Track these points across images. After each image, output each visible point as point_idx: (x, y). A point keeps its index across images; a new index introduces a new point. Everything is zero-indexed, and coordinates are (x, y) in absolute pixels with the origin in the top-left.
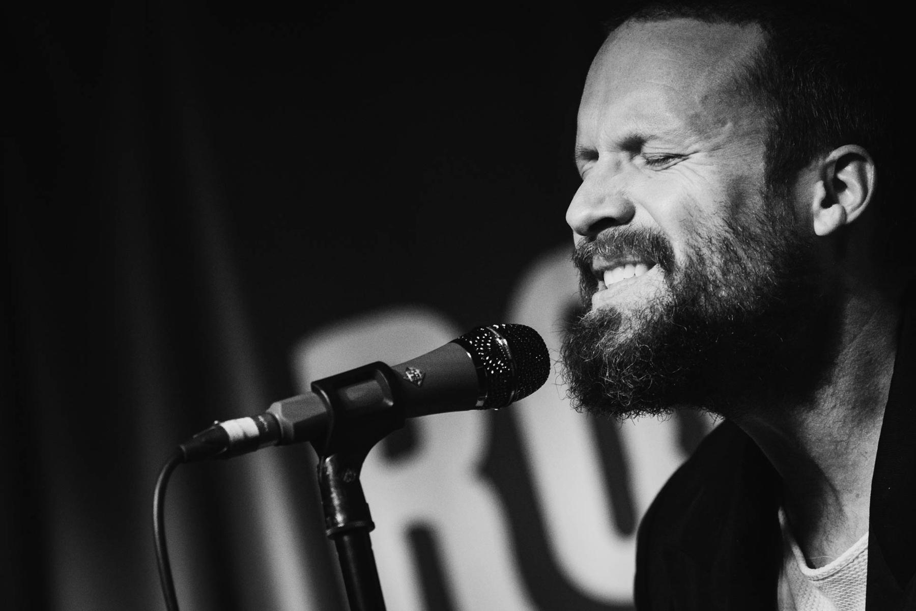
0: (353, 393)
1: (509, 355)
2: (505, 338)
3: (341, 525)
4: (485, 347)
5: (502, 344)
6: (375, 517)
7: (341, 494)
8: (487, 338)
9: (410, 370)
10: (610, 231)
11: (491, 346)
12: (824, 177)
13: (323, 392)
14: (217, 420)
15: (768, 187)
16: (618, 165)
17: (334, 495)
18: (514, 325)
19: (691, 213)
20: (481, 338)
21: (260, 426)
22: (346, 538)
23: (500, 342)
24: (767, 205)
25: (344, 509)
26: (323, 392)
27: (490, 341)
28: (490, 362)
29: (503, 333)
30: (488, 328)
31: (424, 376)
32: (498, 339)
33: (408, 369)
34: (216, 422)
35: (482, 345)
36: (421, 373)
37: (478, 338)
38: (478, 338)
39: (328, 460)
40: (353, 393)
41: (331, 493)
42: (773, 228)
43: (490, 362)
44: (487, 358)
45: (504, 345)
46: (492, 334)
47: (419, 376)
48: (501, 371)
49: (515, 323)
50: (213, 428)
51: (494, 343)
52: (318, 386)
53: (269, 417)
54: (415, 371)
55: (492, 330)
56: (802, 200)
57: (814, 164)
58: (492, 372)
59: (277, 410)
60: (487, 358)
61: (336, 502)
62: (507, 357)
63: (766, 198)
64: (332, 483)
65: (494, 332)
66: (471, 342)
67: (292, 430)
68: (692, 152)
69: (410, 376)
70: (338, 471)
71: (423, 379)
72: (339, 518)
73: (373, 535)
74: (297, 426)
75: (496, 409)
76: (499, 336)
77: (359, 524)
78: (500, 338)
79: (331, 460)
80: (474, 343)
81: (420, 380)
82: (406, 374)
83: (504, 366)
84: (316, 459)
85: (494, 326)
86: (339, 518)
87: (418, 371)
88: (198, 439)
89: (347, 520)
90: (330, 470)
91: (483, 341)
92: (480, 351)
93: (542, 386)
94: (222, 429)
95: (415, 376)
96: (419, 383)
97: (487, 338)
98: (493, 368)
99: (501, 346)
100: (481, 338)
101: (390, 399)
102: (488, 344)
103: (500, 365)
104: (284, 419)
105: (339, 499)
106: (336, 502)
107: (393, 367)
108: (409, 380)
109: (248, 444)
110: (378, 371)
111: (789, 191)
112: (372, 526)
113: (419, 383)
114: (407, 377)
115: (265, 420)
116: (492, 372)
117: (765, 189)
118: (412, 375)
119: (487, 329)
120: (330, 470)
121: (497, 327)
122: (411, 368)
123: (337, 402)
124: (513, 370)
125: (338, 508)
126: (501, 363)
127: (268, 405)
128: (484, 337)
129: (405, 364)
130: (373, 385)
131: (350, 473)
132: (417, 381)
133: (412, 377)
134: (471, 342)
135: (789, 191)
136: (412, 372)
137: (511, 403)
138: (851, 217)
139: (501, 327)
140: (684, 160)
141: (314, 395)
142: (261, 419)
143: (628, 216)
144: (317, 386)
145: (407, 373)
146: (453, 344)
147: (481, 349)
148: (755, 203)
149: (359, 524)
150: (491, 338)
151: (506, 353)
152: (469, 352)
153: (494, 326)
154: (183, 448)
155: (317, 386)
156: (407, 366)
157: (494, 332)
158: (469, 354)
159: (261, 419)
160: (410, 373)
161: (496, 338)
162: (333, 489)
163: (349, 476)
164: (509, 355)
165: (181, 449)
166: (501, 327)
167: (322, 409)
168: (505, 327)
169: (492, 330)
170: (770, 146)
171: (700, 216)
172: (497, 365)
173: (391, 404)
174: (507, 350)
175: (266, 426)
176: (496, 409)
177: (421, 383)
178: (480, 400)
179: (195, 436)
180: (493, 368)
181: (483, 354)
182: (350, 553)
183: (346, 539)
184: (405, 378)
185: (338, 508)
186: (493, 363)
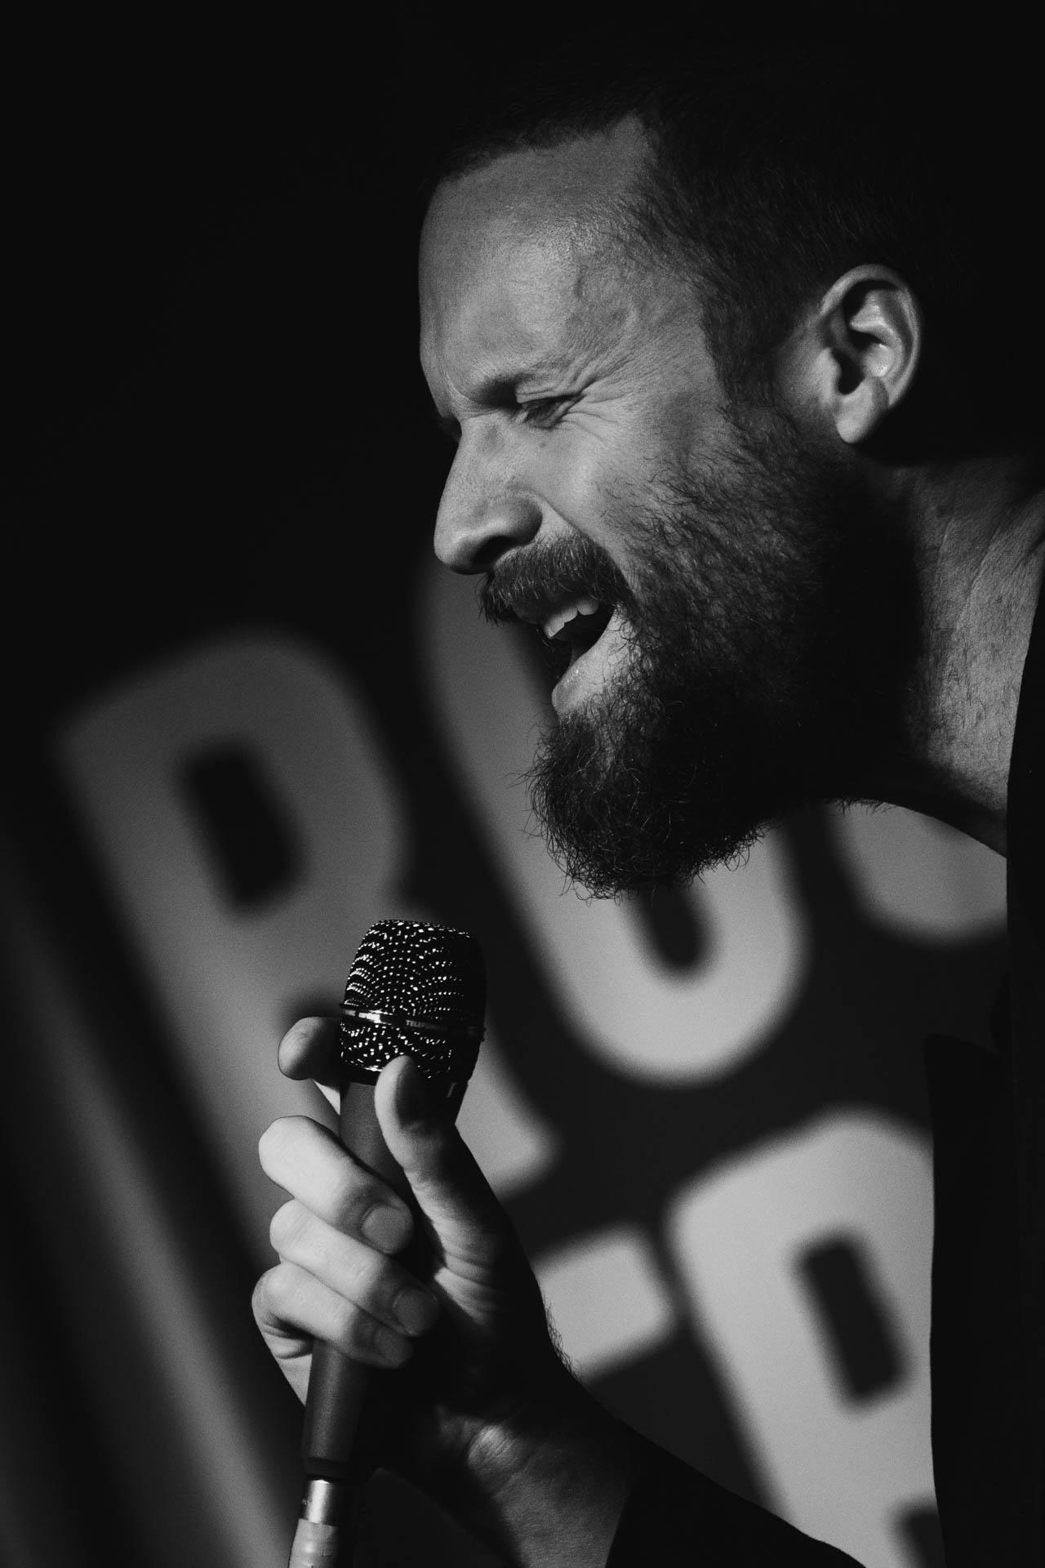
24: (740, 427)
42: (765, 464)
68: (584, 384)
117: (726, 403)
148: (715, 432)
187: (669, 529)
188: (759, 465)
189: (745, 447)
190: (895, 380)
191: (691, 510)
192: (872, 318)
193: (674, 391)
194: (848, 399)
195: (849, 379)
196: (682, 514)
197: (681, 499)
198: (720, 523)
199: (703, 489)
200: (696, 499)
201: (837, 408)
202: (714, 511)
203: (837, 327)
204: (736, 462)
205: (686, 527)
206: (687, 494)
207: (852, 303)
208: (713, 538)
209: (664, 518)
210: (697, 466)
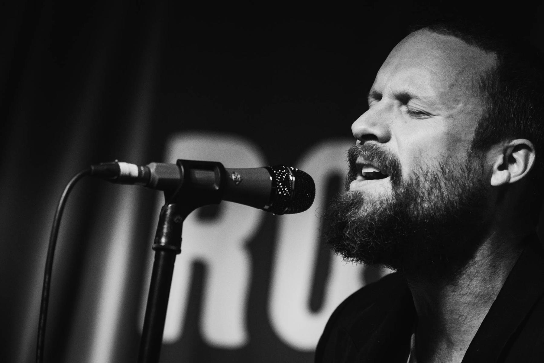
0: (199, 174)
1: (293, 187)
2: (295, 177)
3: (163, 244)
4: (282, 177)
5: (291, 179)
6: (183, 247)
7: (169, 228)
8: (285, 173)
9: (235, 174)
11: (285, 178)
13: (182, 168)
14: (116, 159)
17: (165, 226)
18: (302, 171)
20: (281, 172)
21: (140, 172)
22: (162, 253)
23: (291, 178)
24: (469, 161)
25: (168, 236)
26: (182, 168)
27: (285, 175)
28: (281, 187)
29: (295, 173)
30: (287, 167)
31: (242, 180)
32: (290, 176)
33: (234, 173)
34: (116, 161)
35: (280, 176)
36: (241, 178)
37: (280, 171)
38: (280, 171)
39: (170, 206)
40: (199, 174)
41: (164, 224)
43: (281, 187)
44: (280, 184)
45: (293, 180)
46: (288, 172)
47: (239, 179)
48: (285, 194)
49: (303, 171)
50: (113, 163)
51: (287, 177)
52: (180, 162)
53: (147, 169)
54: (237, 175)
55: (289, 169)
58: (280, 193)
59: (153, 167)
60: (280, 184)
61: (165, 230)
62: (292, 187)
63: (469, 156)
64: (167, 219)
65: (290, 171)
66: (275, 172)
67: (156, 182)
69: (233, 177)
70: (173, 214)
71: (240, 182)
72: (163, 240)
73: (178, 257)
74: (161, 181)
75: (274, 214)
76: (292, 174)
77: (173, 248)
78: (292, 176)
79: (171, 207)
80: (276, 173)
81: (239, 181)
82: (232, 175)
83: (288, 192)
84: (163, 203)
85: (291, 168)
86: (163, 240)
87: (239, 176)
88: (103, 166)
89: (167, 243)
90: (169, 212)
91: (282, 174)
92: (278, 178)
93: (304, 212)
94: (118, 167)
95: (237, 178)
96: (237, 183)
97: (285, 173)
98: (281, 190)
99: (291, 180)
100: (281, 172)
101: (218, 185)
102: (284, 177)
103: (286, 190)
104: (155, 174)
105: (168, 230)
106: (165, 230)
107: (227, 168)
108: (232, 179)
109: (129, 179)
110: (218, 168)
112: (179, 251)
113: (237, 183)
114: (232, 177)
115: (144, 170)
116: (280, 193)
117: (470, 151)
118: (235, 177)
119: (287, 168)
120: (169, 212)
121: (293, 169)
122: (236, 173)
123: (188, 175)
124: (292, 196)
125: (164, 234)
126: (287, 190)
127: (149, 162)
128: (283, 172)
129: (234, 169)
130: (211, 175)
131: (179, 218)
132: (237, 181)
133: (235, 178)
134: (275, 172)
136: (236, 175)
137: (283, 214)
139: (295, 169)
141: (177, 167)
142: (142, 168)
144: (180, 163)
145: (233, 175)
146: (263, 168)
147: (279, 177)
149: (173, 248)
150: (287, 174)
151: (292, 185)
152: (272, 176)
153: (291, 168)
154: (93, 168)
155: (180, 163)
156: (234, 171)
157: (290, 171)
158: (271, 178)
159: (142, 168)
160: (235, 176)
161: (289, 175)
162: (166, 223)
163: (178, 219)
164: (293, 187)
165: (91, 168)
166: (295, 169)
167: (178, 176)
168: (297, 171)
169: (289, 169)
172: (284, 190)
173: (217, 188)
174: (293, 184)
175: (143, 174)
176: (274, 214)
177: (238, 184)
178: (267, 205)
179: (102, 164)
180: (281, 190)
181: (279, 181)
182: (161, 262)
183: (162, 253)
184: (231, 177)
185: (164, 234)
186: (282, 188)
187: (429, 174)
188: (466, 175)
189: (467, 167)
191: (440, 174)
196: (436, 173)
197: (440, 169)
198: (445, 183)
199: (447, 170)
200: (444, 172)
202: (446, 179)
204: (461, 170)
205: (435, 178)
206: (442, 168)
208: (440, 186)
209: (430, 171)
210: (451, 163)
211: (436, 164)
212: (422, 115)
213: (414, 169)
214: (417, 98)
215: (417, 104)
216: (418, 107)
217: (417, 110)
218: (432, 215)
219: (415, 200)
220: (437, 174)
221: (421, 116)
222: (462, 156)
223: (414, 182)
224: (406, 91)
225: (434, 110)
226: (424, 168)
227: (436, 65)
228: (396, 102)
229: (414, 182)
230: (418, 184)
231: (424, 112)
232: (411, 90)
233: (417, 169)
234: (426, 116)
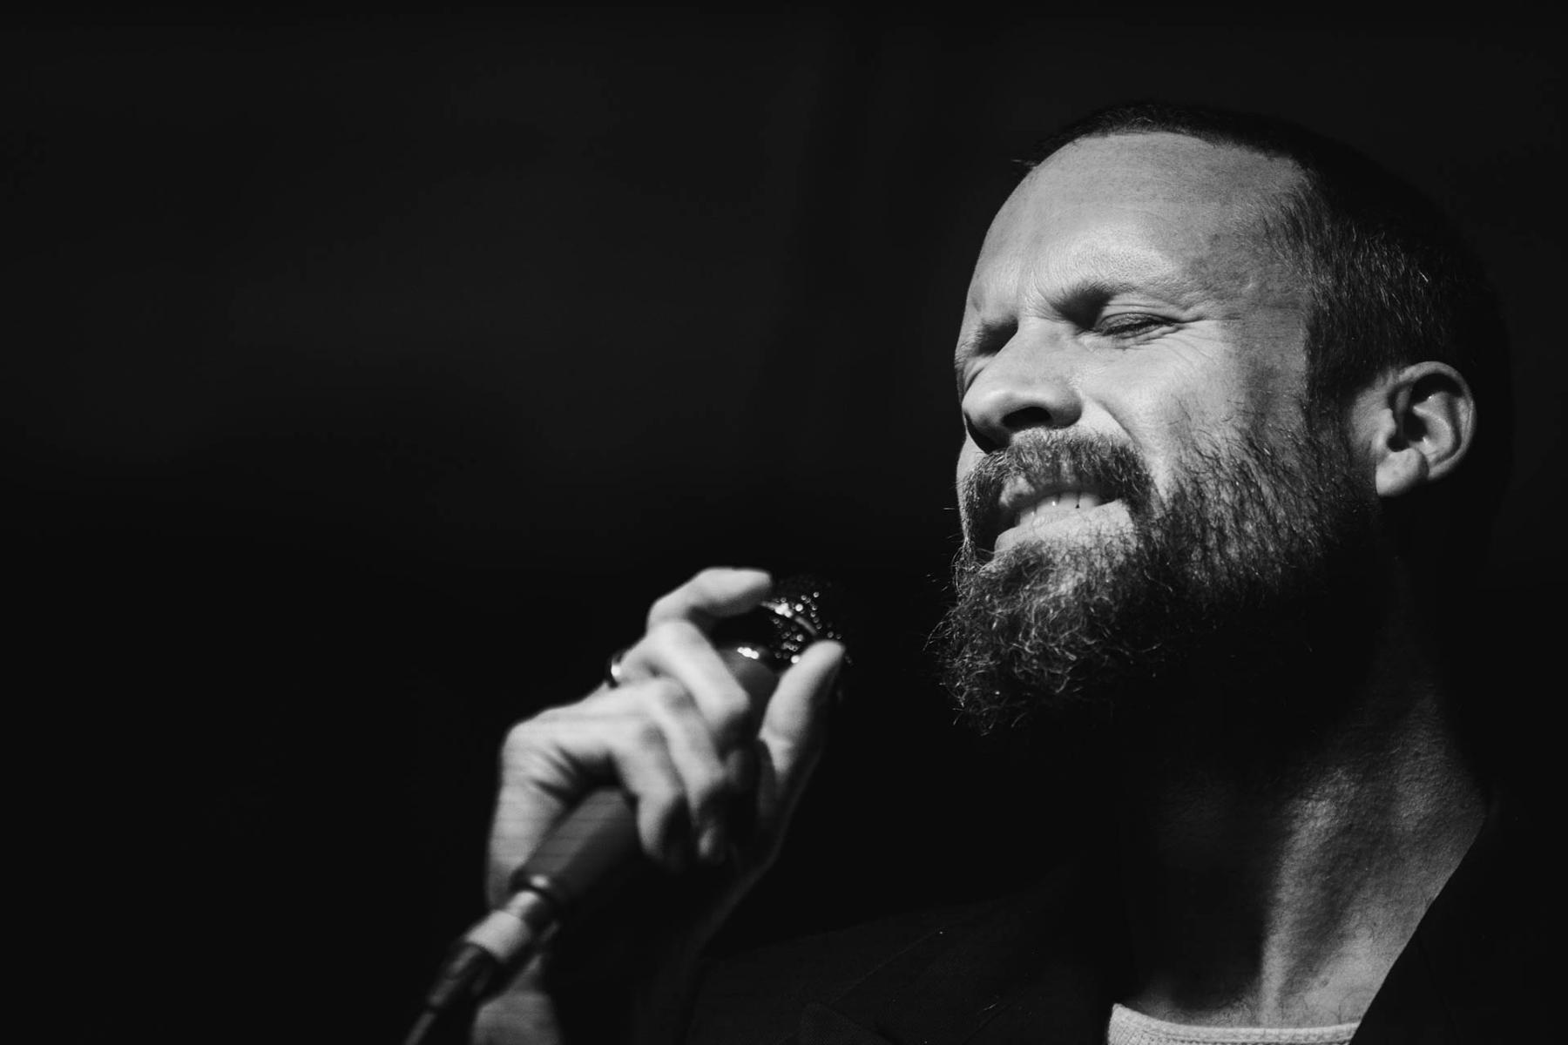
10: (1041, 433)
12: (1391, 401)
15: (1312, 396)
16: (1054, 339)
19: (1190, 414)
56: (1361, 436)
57: (1379, 381)
63: (1308, 414)
111: (1341, 411)
117: (1306, 399)
135: (1341, 411)
138: (1435, 471)
140: (1179, 329)
143: (1069, 416)
170: (1315, 332)
171: (1203, 421)
190: (1439, 460)
191: (1251, 462)
192: (1431, 409)
193: (1268, 363)
194: (1393, 455)
195: (1396, 443)
200: (1259, 458)
201: (1383, 457)
203: (1402, 399)
207: (1420, 390)
211: (1233, 434)
212: (1153, 327)
213: (1181, 457)
214: (1128, 289)
215: (1130, 305)
216: (1137, 309)
217: (1137, 319)
218: (1253, 579)
219: (1203, 541)
220: (1243, 462)
221: (1152, 331)
222: (1289, 418)
223: (1189, 489)
224: (1092, 281)
225: (1186, 308)
226: (1208, 449)
227: (1154, 196)
228: (1063, 328)
229: (1189, 489)
230: (1200, 495)
231: (1159, 319)
232: (1101, 275)
233: (1186, 454)
234: (1165, 328)
